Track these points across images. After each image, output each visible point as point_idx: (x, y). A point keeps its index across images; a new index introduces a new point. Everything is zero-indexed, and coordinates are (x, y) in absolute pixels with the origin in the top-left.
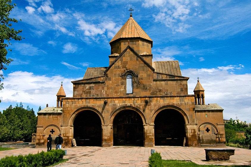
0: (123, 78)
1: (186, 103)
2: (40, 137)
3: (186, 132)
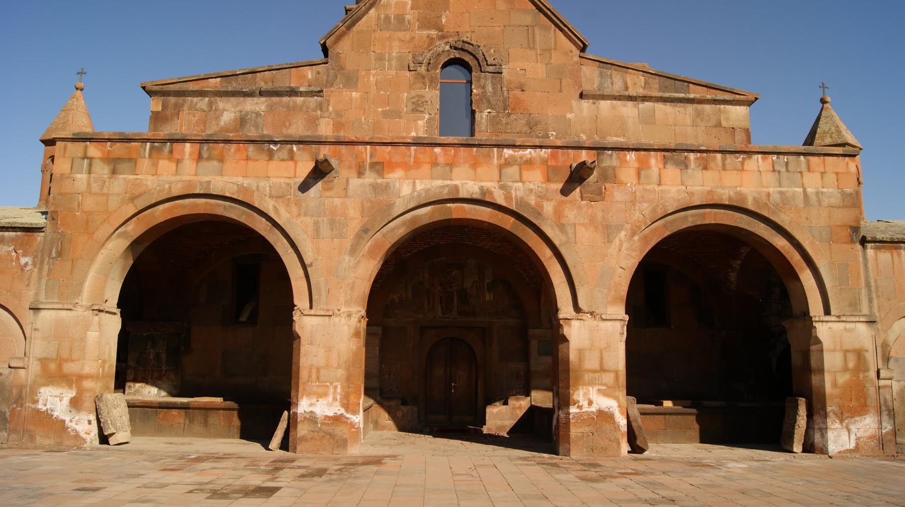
0: (423, 77)
3: (813, 363)
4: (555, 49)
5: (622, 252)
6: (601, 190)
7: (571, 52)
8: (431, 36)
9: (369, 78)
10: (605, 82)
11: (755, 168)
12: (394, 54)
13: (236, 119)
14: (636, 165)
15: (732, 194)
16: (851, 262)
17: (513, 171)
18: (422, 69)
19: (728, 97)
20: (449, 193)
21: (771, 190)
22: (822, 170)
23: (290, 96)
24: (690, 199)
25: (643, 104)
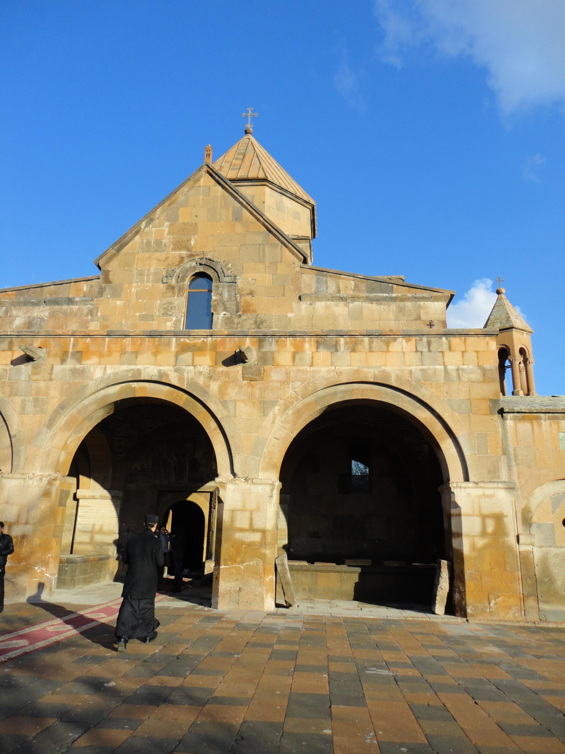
0: (173, 288)
1: (455, 374)
3: (454, 529)
4: (281, 262)
5: (275, 424)
6: (260, 370)
7: (294, 263)
8: (181, 256)
9: (131, 290)
10: (320, 286)
11: (399, 349)
12: (152, 271)
13: (24, 324)
14: (292, 349)
15: (377, 372)
16: (490, 432)
17: (188, 356)
18: (173, 282)
19: (426, 294)
20: (131, 376)
21: (413, 368)
22: (463, 349)
23: (68, 304)
24: (338, 377)
25: (353, 303)
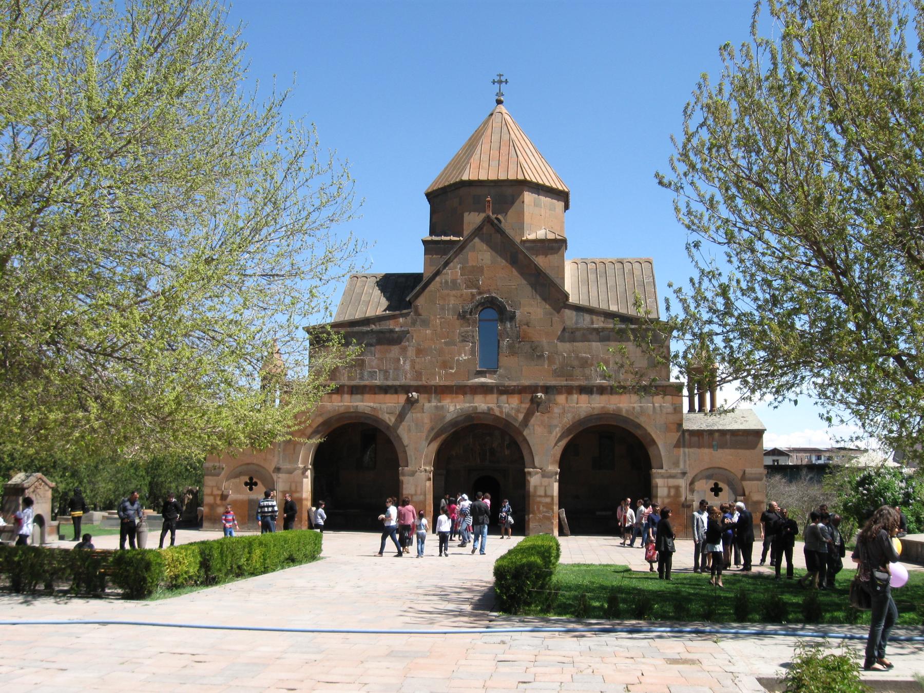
1: (658, 409)
2: (215, 499)
17: (504, 398)
21: (635, 405)
